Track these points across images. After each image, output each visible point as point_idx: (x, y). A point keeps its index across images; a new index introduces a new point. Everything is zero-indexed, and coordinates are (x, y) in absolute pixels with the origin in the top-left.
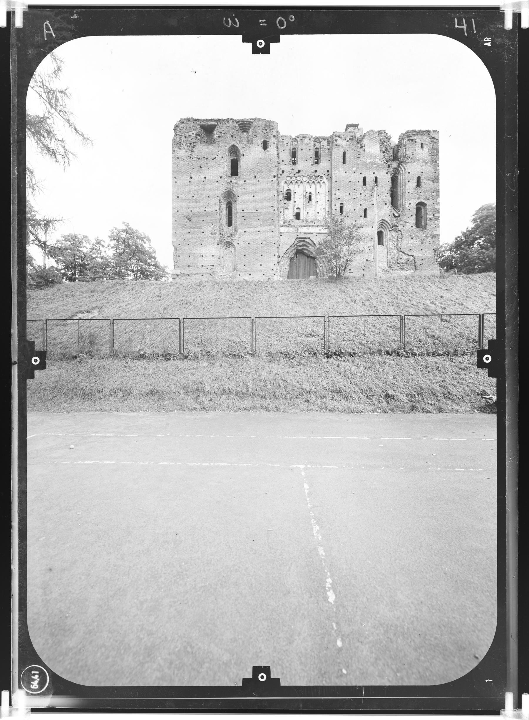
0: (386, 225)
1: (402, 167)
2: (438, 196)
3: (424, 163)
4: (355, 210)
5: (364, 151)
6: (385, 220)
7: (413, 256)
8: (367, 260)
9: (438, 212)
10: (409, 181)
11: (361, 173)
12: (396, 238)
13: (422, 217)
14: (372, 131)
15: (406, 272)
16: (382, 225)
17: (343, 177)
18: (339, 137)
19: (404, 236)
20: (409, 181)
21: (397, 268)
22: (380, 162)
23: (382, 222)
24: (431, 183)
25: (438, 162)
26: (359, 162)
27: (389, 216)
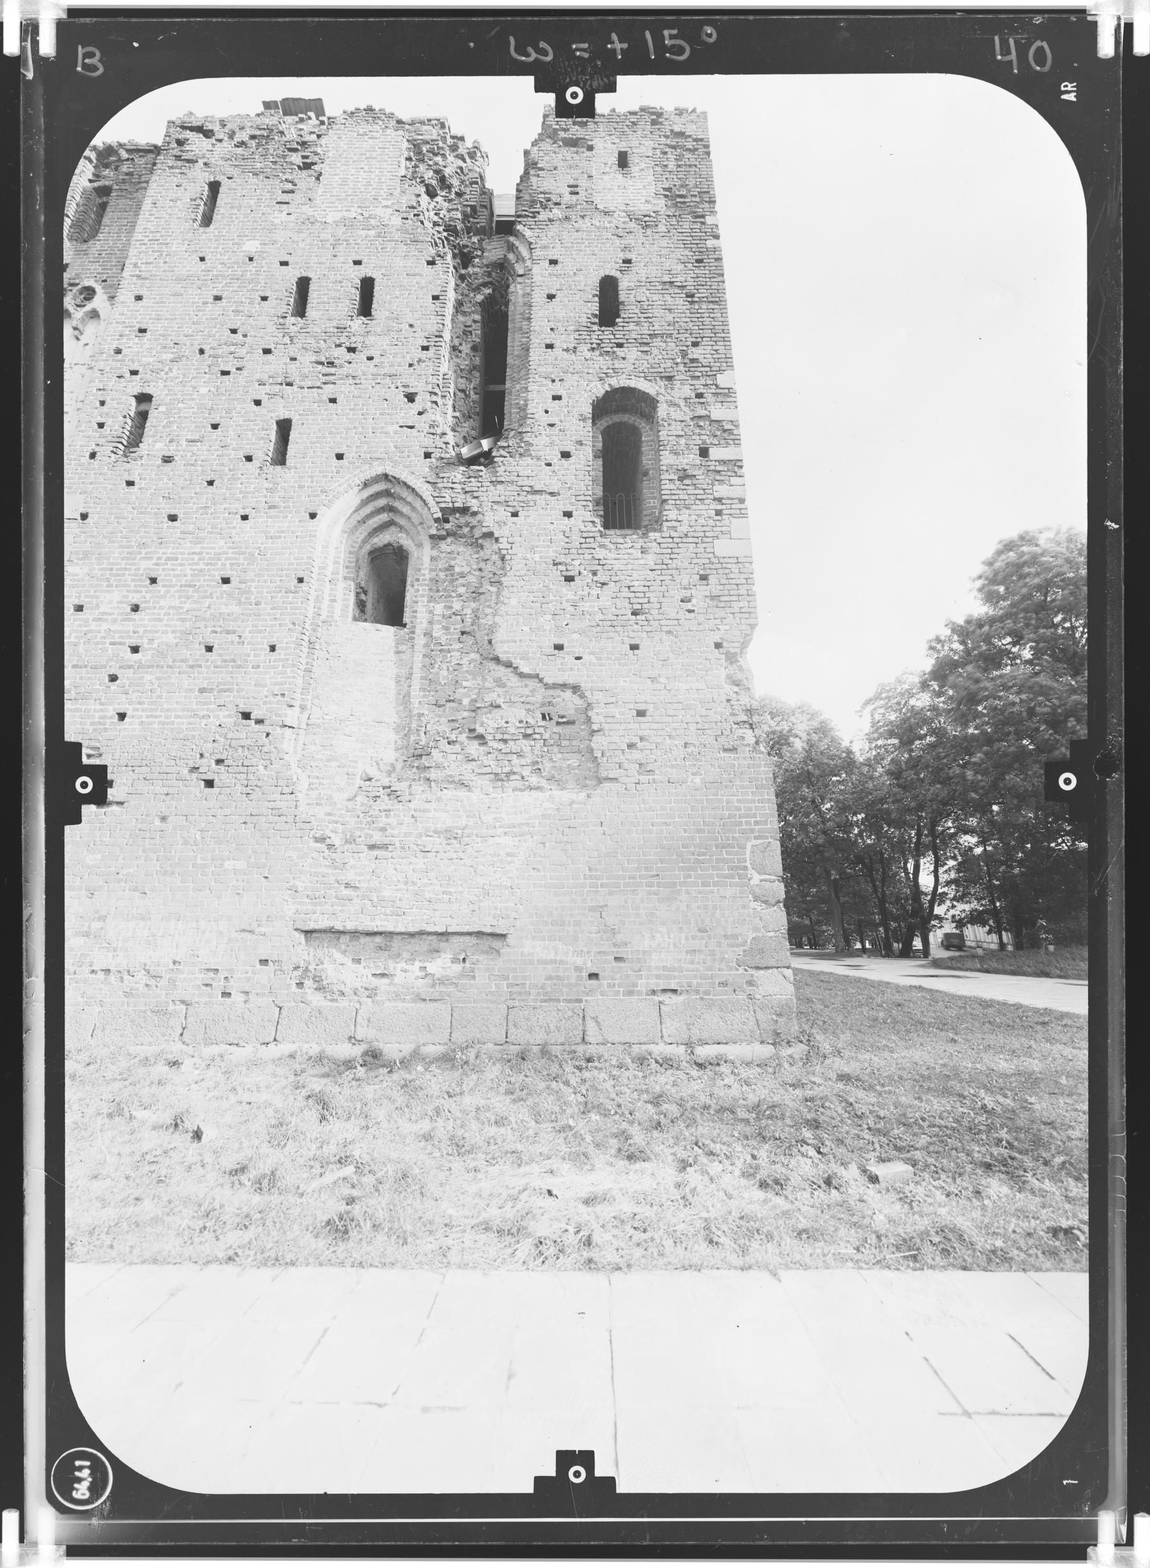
0: (414, 509)
1: (517, 243)
2: (727, 362)
3: (632, 225)
4: (215, 427)
5: (318, 179)
6: (397, 481)
7: (576, 689)
8: (246, 716)
9: (727, 433)
10: (551, 297)
11: (284, 264)
12: (472, 579)
13: (646, 474)
14: (370, 109)
15: (527, 797)
16: (391, 509)
17: (179, 279)
18: (199, 129)
19: (517, 565)
20: (551, 297)
21: (466, 771)
22: (397, 221)
23: (387, 493)
24: (680, 302)
25: (709, 220)
26: (279, 216)
27: (427, 455)
